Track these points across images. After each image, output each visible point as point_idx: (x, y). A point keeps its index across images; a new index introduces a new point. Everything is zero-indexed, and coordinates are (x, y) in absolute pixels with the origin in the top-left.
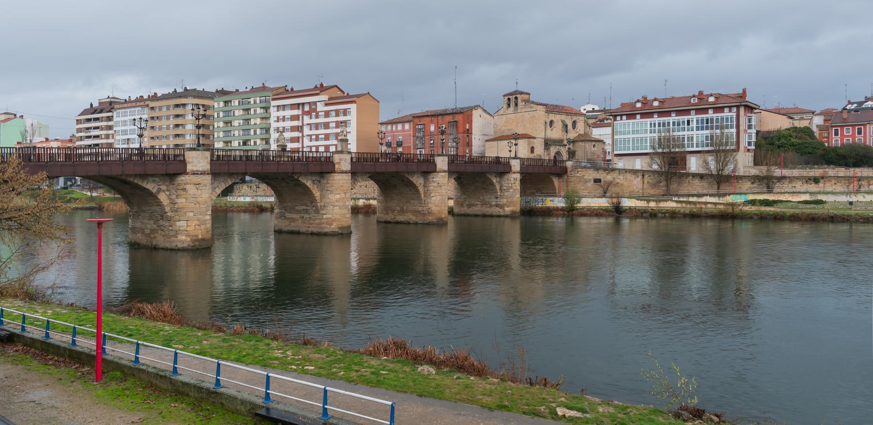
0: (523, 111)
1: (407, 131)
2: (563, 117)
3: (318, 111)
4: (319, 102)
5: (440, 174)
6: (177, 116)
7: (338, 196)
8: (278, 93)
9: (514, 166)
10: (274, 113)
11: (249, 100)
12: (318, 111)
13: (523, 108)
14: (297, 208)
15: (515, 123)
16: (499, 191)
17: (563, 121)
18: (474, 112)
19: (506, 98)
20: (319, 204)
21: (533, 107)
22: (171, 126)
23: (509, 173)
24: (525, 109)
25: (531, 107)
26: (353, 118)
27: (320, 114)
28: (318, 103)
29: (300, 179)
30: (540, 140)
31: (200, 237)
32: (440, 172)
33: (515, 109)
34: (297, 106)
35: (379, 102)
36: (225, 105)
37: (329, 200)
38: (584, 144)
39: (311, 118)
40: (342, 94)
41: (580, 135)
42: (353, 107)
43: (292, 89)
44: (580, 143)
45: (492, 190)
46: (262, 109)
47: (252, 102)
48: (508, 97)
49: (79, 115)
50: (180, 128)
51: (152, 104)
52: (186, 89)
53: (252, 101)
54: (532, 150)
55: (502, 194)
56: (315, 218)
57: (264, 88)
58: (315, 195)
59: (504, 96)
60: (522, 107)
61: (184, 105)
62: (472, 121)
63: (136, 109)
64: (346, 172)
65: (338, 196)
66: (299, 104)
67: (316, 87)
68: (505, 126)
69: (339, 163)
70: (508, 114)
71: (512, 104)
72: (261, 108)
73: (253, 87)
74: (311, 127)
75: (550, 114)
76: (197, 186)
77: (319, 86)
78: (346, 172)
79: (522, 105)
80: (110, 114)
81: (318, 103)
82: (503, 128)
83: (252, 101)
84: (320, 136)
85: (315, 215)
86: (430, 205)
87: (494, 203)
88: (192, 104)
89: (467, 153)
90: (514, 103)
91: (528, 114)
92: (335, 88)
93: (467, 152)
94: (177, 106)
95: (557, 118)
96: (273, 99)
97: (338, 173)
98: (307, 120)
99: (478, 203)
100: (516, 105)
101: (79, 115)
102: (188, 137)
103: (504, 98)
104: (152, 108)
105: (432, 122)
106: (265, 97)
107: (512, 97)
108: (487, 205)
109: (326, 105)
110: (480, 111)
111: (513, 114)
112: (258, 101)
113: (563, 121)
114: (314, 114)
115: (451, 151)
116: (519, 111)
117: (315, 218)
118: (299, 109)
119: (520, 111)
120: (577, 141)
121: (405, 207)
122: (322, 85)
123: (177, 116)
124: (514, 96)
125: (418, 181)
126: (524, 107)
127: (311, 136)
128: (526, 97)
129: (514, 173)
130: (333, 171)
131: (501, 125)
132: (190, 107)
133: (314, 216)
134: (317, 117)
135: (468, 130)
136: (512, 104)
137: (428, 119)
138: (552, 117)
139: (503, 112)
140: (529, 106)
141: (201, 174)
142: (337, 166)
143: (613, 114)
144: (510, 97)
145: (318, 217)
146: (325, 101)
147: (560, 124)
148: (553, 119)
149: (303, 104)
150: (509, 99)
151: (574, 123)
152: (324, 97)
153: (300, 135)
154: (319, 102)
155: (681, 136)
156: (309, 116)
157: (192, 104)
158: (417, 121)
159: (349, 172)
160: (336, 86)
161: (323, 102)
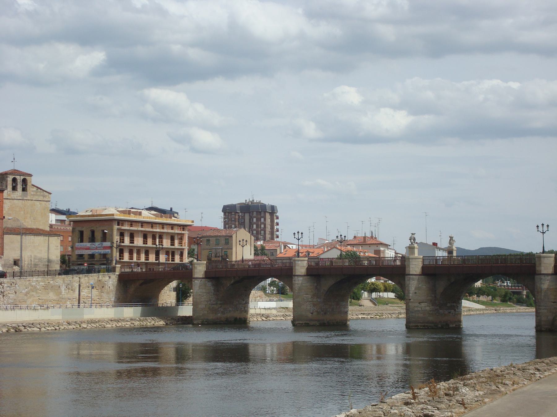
13: (34, 195)
15: (22, 212)
21: (47, 196)
48: (14, 176)
60: (32, 193)
71: (20, 187)
79: (33, 191)
91: (40, 204)
119: (29, 198)
124: (22, 177)
126: (35, 193)
136: (20, 187)
140: (42, 194)
144: (18, 177)
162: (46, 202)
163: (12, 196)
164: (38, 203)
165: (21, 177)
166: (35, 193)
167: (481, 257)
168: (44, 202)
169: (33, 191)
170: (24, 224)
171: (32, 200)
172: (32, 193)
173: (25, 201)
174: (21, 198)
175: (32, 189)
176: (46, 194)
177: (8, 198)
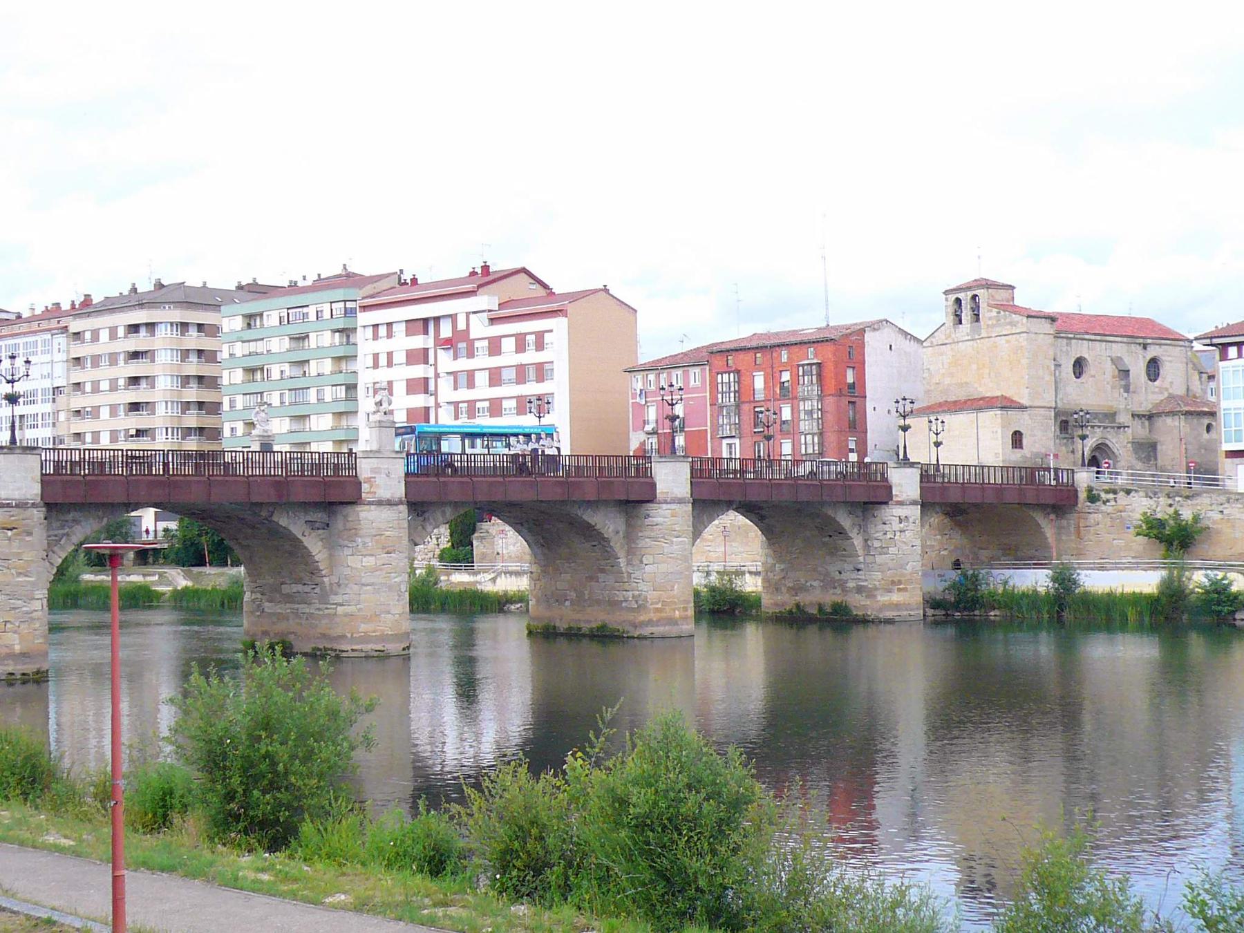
0: (998, 331)
1: (695, 390)
2: (1119, 349)
3: (472, 337)
4: (474, 313)
5: (665, 506)
7: (369, 561)
8: (376, 291)
9: (900, 485)
10: (365, 345)
11: (305, 310)
12: (472, 337)
13: (993, 326)
14: (286, 589)
15: (974, 367)
16: (860, 552)
17: (1116, 361)
19: (952, 297)
20: (326, 580)
22: (121, 382)
23: (886, 503)
24: (998, 329)
25: (1012, 324)
27: (477, 344)
28: (472, 316)
29: (275, 518)
30: (1042, 411)
31: (17, 648)
32: (666, 502)
33: (973, 331)
35: (636, 311)
36: (249, 325)
37: (347, 571)
38: (1177, 424)
39: (456, 358)
40: (543, 292)
41: (1171, 397)
42: (557, 328)
43: (414, 281)
44: (1169, 420)
45: (845, 550)
46: (337, 334)
47: (312, 317)
50: (143, 384)
51: (75, 325)
52: (160, 286)
53: (312, 311)
54: (1017, 439)
55: (869, 559)
56: (321, 613)
57: (348, 279)
58: (316, 558)
59: (946, 293)
61: (151, 326)
62: (863, 363)
63: (38, 338)
64: (390, 503)
66: (426, 321)
67: (473, 273)
68: (952, 375)
69: (369, 480)
70: (958, 342)
71: (966, 315)
72: (334, 331)
73: (319, 275)
74: (456, 382)
75: (1073, 341)
76: (9, 533)
77: (479, 271)
78: (390, 503)
79: (990, 319)
81: (472, 316)
82: (947, 381)
83: (312, 311)
84: (506, 404)
85: (321, 606)
86: (642, 586)
87: (851, 584)
88: (172, 324)
89: (852, 451)
90: (970, 313)
91: (1008, 342)
92: (523, 275)
93: (852, 445)
94: (134, 328)
95: (1098, 354)
96: (364, 308)
97: (370, 503)
98: (446, 361)
99: (815, 584)
100: (976, 317)
102: (161, 410)
103: (947, 300)
104: (77, 335)
105: (756, 366)
106: (345, 301)
107: (965, 297)
108: (835, 588)
109: (493, 321)
110: (887, 335)
111: (969, 343)
112: (327, 315)
113: (1116, 361)
114: (462, 345)
115: (806, 444)
116: (984, 334)
117: (321, 613)
118: (426, 332)
119: (984, 334)
120: (1159, 414)
121: (586, 592)
122: (486, 268)
123: (135, 355)
124: (970, 294)
125: (609, 524)
126: (995, 322)
127: (456, 404)
128: (1001, 295)
129: (901, 503)
130: (356, 500)
131: (942, 371)
132: (161, 331)
133: (319, 609)
134: (471, 354)
135: (852, 386)
136: (966, 315)
137: (748, 357)
138: (1081, 349)
139: (944, 337)
140: (1008, 320)
141: (17, 506)
142: (365, 487)
143: (1215, 341)
144: (961, 296)
145: (326, 612)
146: (490, 311)
147: (1110, 368)
148: (1086, 356)
149: (437, 320)
150: (958, 301)
151: (1153, 368)
152: (486, 301)
153: (431, 402)
154: (474, 313)
155: (1233, 412)
156: (452, 351)
157: (172, 324)
158: (719, 362)
159: (400, 503)
161: (485, 314)
162: (1018, 336)
163: (953, 336)
164: (1003, 340)
165: (968, 293)
166: (995, 322)
167: (295, 454)
168: (1014, 336)
169: (990, 319)
170: (980, 389)
171: (991, 337)
172: (990, 323)
173: (978, 341)
174: (969, 338)
175: (988, 315)
176: (1016, 319)
177: (947, 342)
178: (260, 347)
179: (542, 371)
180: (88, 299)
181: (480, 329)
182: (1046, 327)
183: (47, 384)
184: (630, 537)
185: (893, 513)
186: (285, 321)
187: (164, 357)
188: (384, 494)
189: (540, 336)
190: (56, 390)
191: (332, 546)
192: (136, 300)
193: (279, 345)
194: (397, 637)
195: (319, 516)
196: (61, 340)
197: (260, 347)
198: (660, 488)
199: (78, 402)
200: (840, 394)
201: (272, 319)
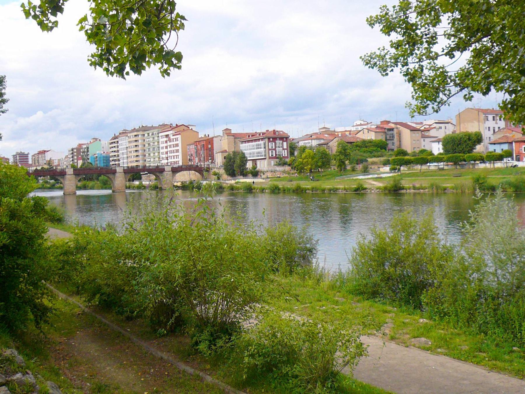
6: (136, 141)
7: (68, 182)
18: (214, 139)
26: (179, 142)
34: (167, 136)
42: (179, 137)
49: (110, 140)
52: (143, 126)
57: (164, 125)
61: (138, 135)
65: (68, 182)
80: (117, 140)
92: (183, 126)
94: (136, 136)
98: (169, 144)
101: (110, 140)
102: (140, 151)
104: (129, 137)
109: (173, 135)
118: (167, 137)
123: (136, 141)
130: (66, 175)
132: (140, 136)
160: (183, 125)
178: (149, 140)
179: (177, 145)
180: (135, 129)
181: (172, 137)
182: (232, 137)
183: (126, 146)
184: (114, 178)
185: (165, 173)
186: (153, 134)
187: (140, 141)
188: (69, 174)
189: (178, 138)
190: (127, 147)
191: (64, 180)
192: (134, 130)
193: (151, 139)
194: (72, 192)
195: (62, 176)
196: (127, 138)
197: (149, 140)
198: (117, 171)
199: (129, 150)
200: (206, 150)
201: (150, 134)
